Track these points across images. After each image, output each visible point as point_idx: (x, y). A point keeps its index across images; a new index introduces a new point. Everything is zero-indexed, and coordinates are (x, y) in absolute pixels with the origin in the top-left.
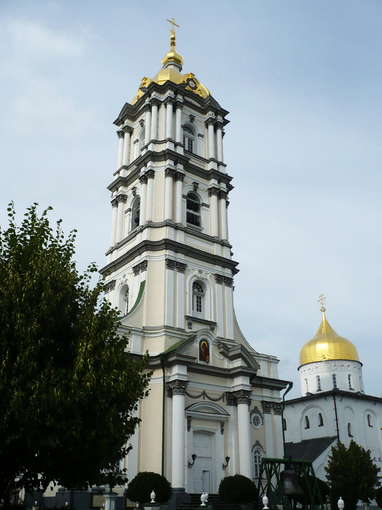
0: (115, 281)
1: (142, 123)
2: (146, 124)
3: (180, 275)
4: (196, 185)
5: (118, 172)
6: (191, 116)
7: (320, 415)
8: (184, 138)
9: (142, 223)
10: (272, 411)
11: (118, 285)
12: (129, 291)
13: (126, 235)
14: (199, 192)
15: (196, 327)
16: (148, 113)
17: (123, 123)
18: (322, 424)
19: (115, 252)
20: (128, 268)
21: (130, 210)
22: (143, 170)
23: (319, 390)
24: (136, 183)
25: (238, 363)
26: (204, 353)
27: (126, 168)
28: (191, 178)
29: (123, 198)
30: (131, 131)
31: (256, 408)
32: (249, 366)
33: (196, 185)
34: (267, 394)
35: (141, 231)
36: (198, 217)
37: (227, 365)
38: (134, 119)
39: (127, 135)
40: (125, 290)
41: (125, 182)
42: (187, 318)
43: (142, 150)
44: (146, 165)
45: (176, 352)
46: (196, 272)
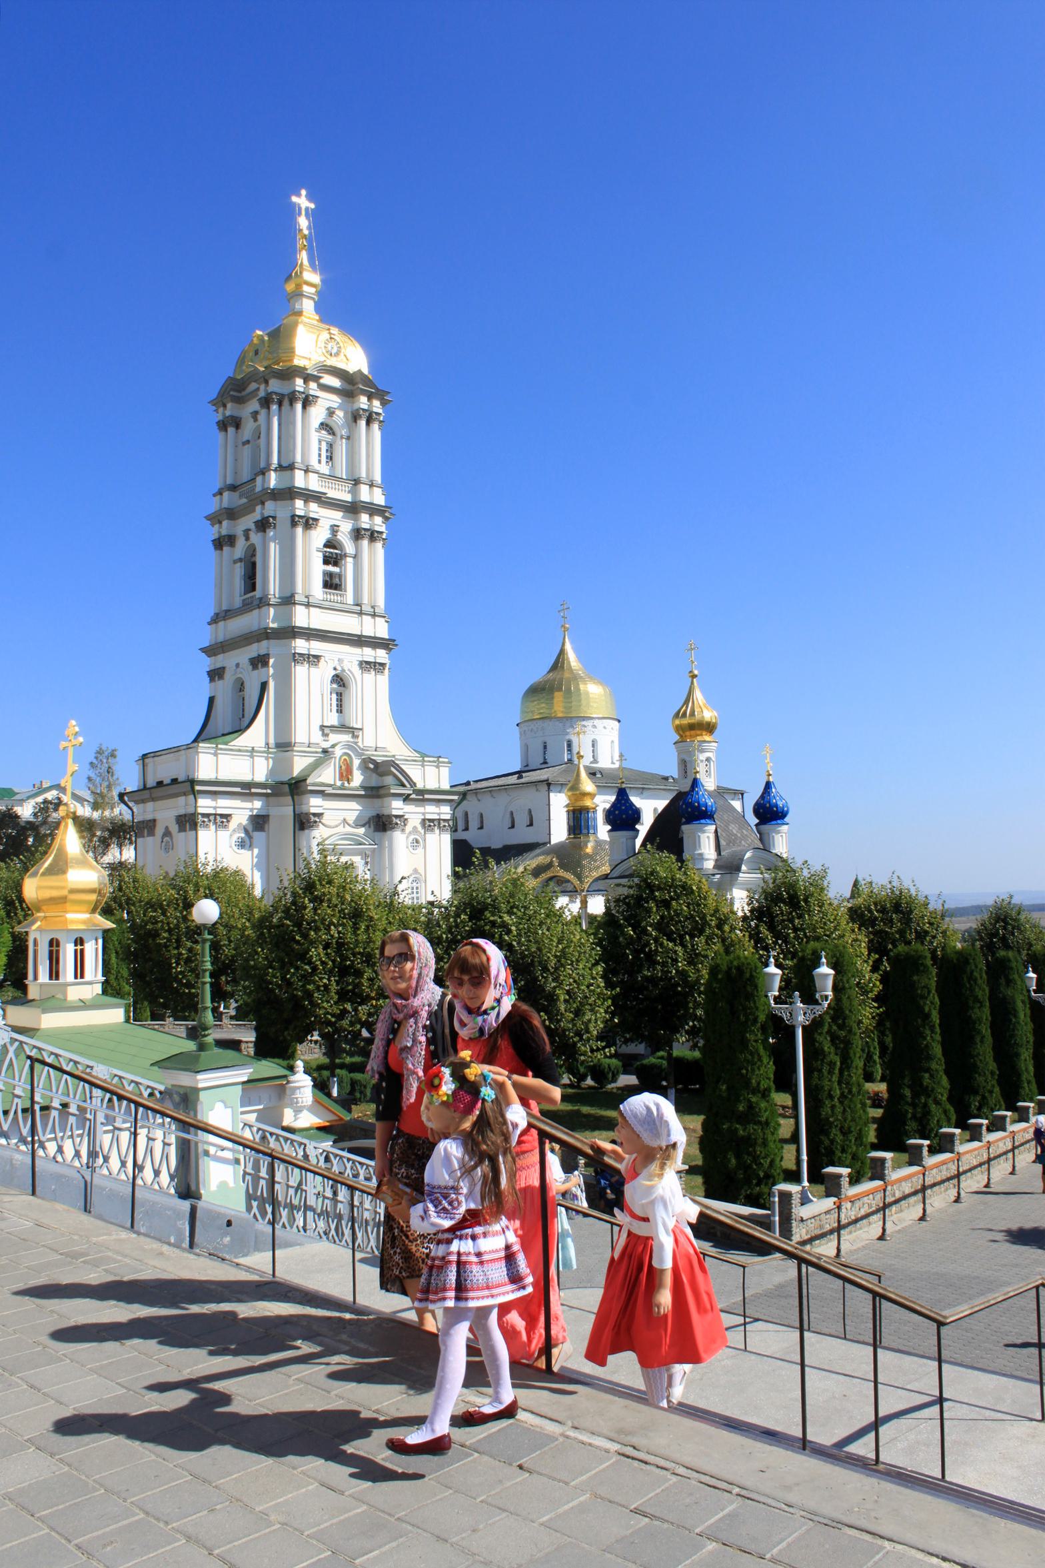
0: (224, 668)
1: (255, 415)
2: (262, 417)
3: (313, 669)
4: (334, 529)
5: (220, 493)
6: (328, 409)
7: (530, 811)
8: (320, 442)
9: (258, 593)
10: (437, 831)
11: (228, 676)
12: (247, 685)
13: (238, 602)
14: (340, 536)
15: (334, 738)
16: (263, 412)
17: (225, 406)
18: (531, 824)
19: (221, 624)
20: (243, 656)
21: (240, 560)
22: (258, 508)
23: (545, 763)
24: (248, 522)
25: (389, 780)
26: (346, 774)
27: (233, 488)
28: (328, 517)
29: (230, 540)
30: (237, 423)
31: (415, 828)
32: (403, 785)
33: (334, 529)
34: (432, 811)
35: (259, 608)
36: (340, 576)
37: (374, 781)
38: (240, 401)
39: (231, 430)
40: (241, 686)
41: (231, 514)
42: (322, 727)
43: (257, 475)
44: (263, 503)
45: (308, 781)
46: (336, 664)
